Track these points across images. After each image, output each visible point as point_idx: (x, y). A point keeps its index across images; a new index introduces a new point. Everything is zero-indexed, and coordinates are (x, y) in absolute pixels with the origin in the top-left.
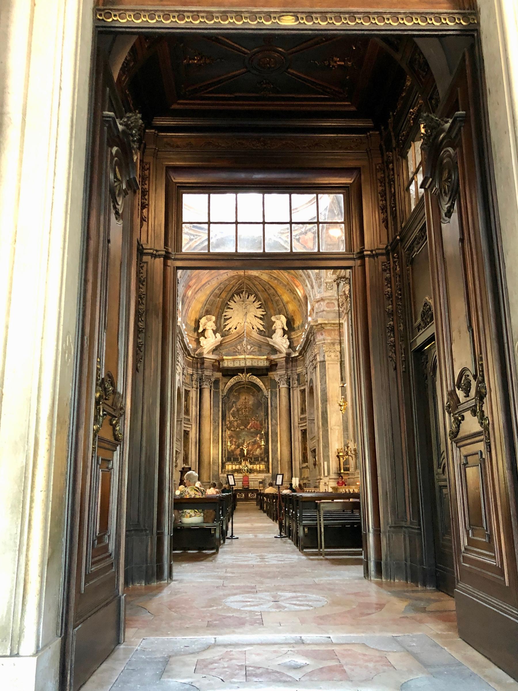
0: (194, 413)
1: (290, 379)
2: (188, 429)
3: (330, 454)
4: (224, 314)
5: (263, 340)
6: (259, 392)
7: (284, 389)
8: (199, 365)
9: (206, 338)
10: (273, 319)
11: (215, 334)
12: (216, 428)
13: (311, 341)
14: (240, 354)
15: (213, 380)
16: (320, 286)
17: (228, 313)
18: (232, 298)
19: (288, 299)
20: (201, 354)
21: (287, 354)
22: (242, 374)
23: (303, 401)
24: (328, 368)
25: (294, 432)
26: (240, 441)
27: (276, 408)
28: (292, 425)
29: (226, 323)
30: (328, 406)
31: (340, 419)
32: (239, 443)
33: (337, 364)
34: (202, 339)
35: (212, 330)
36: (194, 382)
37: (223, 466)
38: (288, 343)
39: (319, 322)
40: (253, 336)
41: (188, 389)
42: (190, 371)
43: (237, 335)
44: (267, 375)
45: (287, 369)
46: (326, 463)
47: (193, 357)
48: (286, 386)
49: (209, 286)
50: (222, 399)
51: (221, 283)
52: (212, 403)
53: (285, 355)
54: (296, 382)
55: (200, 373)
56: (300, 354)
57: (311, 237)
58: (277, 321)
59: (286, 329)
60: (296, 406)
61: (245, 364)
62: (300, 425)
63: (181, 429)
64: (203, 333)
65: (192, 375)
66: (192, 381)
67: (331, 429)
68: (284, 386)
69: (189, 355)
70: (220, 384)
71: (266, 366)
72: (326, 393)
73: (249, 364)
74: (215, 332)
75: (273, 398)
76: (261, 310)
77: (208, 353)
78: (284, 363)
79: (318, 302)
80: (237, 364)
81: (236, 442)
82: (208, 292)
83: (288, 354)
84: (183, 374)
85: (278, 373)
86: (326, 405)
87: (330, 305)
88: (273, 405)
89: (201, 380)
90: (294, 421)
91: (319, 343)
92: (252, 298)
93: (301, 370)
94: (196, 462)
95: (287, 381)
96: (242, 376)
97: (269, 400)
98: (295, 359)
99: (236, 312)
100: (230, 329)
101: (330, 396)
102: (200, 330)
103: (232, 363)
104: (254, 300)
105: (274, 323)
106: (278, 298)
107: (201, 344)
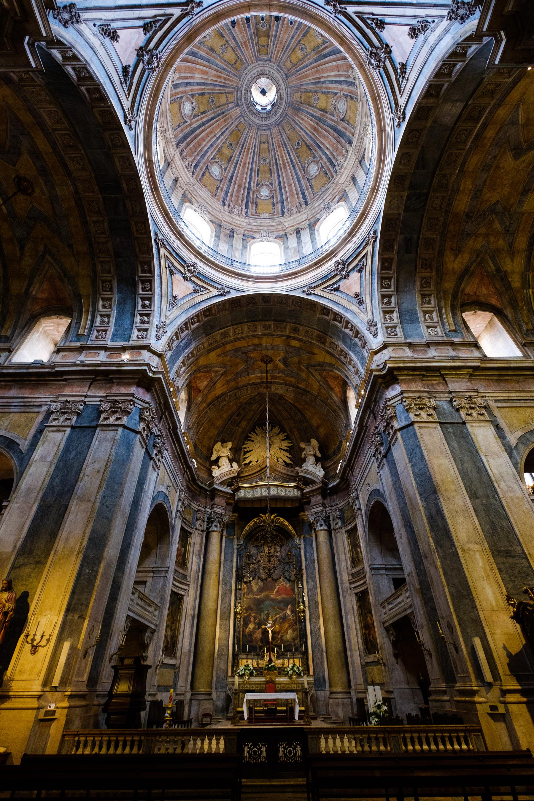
0: (195, 568)
1: (329, 518)
2: (183, 593)
3: (482, 616)
4: (244, 446)
5: (290, 474)
6: (287, 539)
7: (322, 532)
8: (208, 501)
9: (219, 467)
10: (302, 445)
11: (231, 464)
12: (227, 593)
13: (367, 427)
14: (261, 480)
15: (225, 520)
16: (375, 335)
17: (248, 445)
18: (253, 430)
19: (319, 422)
20: (212, 484)
21: (323, 482)
22: (265, 515)
23: (355, 545)
24: (421, 434)
25: (344, 598)
26: (263, 616)
27: (313, 562)
28: (340, 587)
29: (246, 456)
30: (441, 499)
31: (475, 528)
32: (260, 620)
33: (435, 427)
34: (215, 467)
35: (229, 459)
36: (198, 522)
37: (235, 663)
38: (324, 472)
39: (388, 365)
40: (279, 469)
41: (189, 530)
42: (195, 506)
43: (259, 469)
44: (298, 516)
45: (324, 505)
46: (477, 642)
47: (202, 488)
48: (324, 527)
49: (224, 403)
50: (238, 549)
51: (240, 407)
52: (223, 554)
53: (321, 485)
54: (339, 521)
55: (210, 511)
56: (342, 479)
57: (356, 278)
58: (306, 447)
59: (319, 455)
60: (342, 557)
61: (269, 492)
62: (353, 586)
63: (164, 585)
64: (216, 462)
65: (197, 511)
66: (197, 520)
67: (463, 550)
68: (322, 528)
69: (194, 480)
70: (236, 528)
71: (297, 496)
72: (430, 478)
73: (274, 492)
74: (231, 461)
75: (308, 549)
76: (286, 441)
77: (222, 483)
78: (320, 497)
79: (376, 353)
80: (257, 493)
81: (255, 618)
82: (225, 416)
83: (324, 483)
84: (180, 500)
85: (313, 510)
86: (436, 499)
87: (399, 351)
88: (308, 557)
89: (210, 521)
90: (342, 580)
91: (392, 402)
92: (276, 430)
93: (345, 502)
94: (190, 652)
95: (325, 521)
96: (264, 518)
97: (302, 551)
98: (335, 490)
99: (258, 445)
100: (250, 462)
101: (439, 481)
102: (213, 458)
103: (251, 492)
104: (278, 432)
105: (304, 449)
106: (305, 424)
107: (213, 475)
